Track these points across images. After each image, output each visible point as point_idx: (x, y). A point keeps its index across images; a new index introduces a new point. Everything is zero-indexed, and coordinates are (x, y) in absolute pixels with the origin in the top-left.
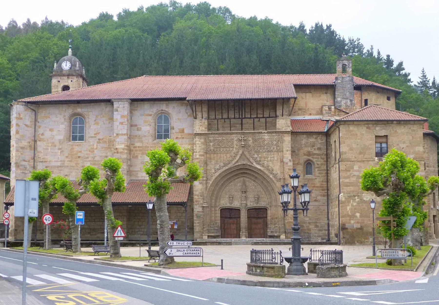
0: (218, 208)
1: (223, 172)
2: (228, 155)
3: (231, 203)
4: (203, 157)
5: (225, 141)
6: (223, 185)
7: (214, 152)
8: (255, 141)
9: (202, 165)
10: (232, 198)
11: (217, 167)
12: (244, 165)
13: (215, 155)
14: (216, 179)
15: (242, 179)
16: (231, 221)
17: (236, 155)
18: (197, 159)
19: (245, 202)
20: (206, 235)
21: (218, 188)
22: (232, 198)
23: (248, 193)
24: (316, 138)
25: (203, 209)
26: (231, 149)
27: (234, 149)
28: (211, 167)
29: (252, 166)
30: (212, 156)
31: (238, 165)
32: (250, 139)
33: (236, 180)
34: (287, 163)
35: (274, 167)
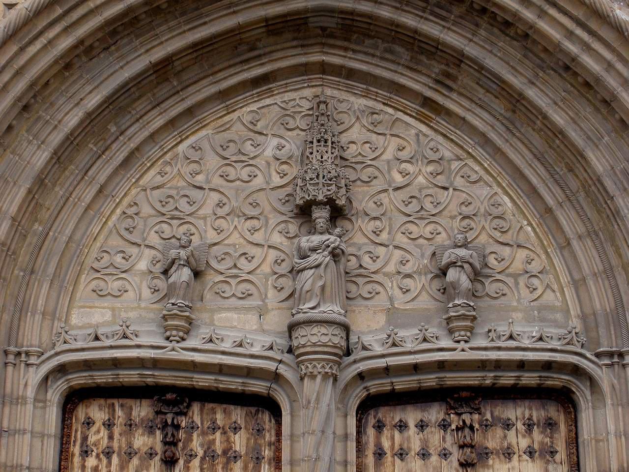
0: (35, 376)
3: (178, 323)
6: (95, 124)
10: (189, 273)
15: (300, 96)
19: (332, 309)
21: (41, 158)
22: (189, 273)
23: (358, 235)
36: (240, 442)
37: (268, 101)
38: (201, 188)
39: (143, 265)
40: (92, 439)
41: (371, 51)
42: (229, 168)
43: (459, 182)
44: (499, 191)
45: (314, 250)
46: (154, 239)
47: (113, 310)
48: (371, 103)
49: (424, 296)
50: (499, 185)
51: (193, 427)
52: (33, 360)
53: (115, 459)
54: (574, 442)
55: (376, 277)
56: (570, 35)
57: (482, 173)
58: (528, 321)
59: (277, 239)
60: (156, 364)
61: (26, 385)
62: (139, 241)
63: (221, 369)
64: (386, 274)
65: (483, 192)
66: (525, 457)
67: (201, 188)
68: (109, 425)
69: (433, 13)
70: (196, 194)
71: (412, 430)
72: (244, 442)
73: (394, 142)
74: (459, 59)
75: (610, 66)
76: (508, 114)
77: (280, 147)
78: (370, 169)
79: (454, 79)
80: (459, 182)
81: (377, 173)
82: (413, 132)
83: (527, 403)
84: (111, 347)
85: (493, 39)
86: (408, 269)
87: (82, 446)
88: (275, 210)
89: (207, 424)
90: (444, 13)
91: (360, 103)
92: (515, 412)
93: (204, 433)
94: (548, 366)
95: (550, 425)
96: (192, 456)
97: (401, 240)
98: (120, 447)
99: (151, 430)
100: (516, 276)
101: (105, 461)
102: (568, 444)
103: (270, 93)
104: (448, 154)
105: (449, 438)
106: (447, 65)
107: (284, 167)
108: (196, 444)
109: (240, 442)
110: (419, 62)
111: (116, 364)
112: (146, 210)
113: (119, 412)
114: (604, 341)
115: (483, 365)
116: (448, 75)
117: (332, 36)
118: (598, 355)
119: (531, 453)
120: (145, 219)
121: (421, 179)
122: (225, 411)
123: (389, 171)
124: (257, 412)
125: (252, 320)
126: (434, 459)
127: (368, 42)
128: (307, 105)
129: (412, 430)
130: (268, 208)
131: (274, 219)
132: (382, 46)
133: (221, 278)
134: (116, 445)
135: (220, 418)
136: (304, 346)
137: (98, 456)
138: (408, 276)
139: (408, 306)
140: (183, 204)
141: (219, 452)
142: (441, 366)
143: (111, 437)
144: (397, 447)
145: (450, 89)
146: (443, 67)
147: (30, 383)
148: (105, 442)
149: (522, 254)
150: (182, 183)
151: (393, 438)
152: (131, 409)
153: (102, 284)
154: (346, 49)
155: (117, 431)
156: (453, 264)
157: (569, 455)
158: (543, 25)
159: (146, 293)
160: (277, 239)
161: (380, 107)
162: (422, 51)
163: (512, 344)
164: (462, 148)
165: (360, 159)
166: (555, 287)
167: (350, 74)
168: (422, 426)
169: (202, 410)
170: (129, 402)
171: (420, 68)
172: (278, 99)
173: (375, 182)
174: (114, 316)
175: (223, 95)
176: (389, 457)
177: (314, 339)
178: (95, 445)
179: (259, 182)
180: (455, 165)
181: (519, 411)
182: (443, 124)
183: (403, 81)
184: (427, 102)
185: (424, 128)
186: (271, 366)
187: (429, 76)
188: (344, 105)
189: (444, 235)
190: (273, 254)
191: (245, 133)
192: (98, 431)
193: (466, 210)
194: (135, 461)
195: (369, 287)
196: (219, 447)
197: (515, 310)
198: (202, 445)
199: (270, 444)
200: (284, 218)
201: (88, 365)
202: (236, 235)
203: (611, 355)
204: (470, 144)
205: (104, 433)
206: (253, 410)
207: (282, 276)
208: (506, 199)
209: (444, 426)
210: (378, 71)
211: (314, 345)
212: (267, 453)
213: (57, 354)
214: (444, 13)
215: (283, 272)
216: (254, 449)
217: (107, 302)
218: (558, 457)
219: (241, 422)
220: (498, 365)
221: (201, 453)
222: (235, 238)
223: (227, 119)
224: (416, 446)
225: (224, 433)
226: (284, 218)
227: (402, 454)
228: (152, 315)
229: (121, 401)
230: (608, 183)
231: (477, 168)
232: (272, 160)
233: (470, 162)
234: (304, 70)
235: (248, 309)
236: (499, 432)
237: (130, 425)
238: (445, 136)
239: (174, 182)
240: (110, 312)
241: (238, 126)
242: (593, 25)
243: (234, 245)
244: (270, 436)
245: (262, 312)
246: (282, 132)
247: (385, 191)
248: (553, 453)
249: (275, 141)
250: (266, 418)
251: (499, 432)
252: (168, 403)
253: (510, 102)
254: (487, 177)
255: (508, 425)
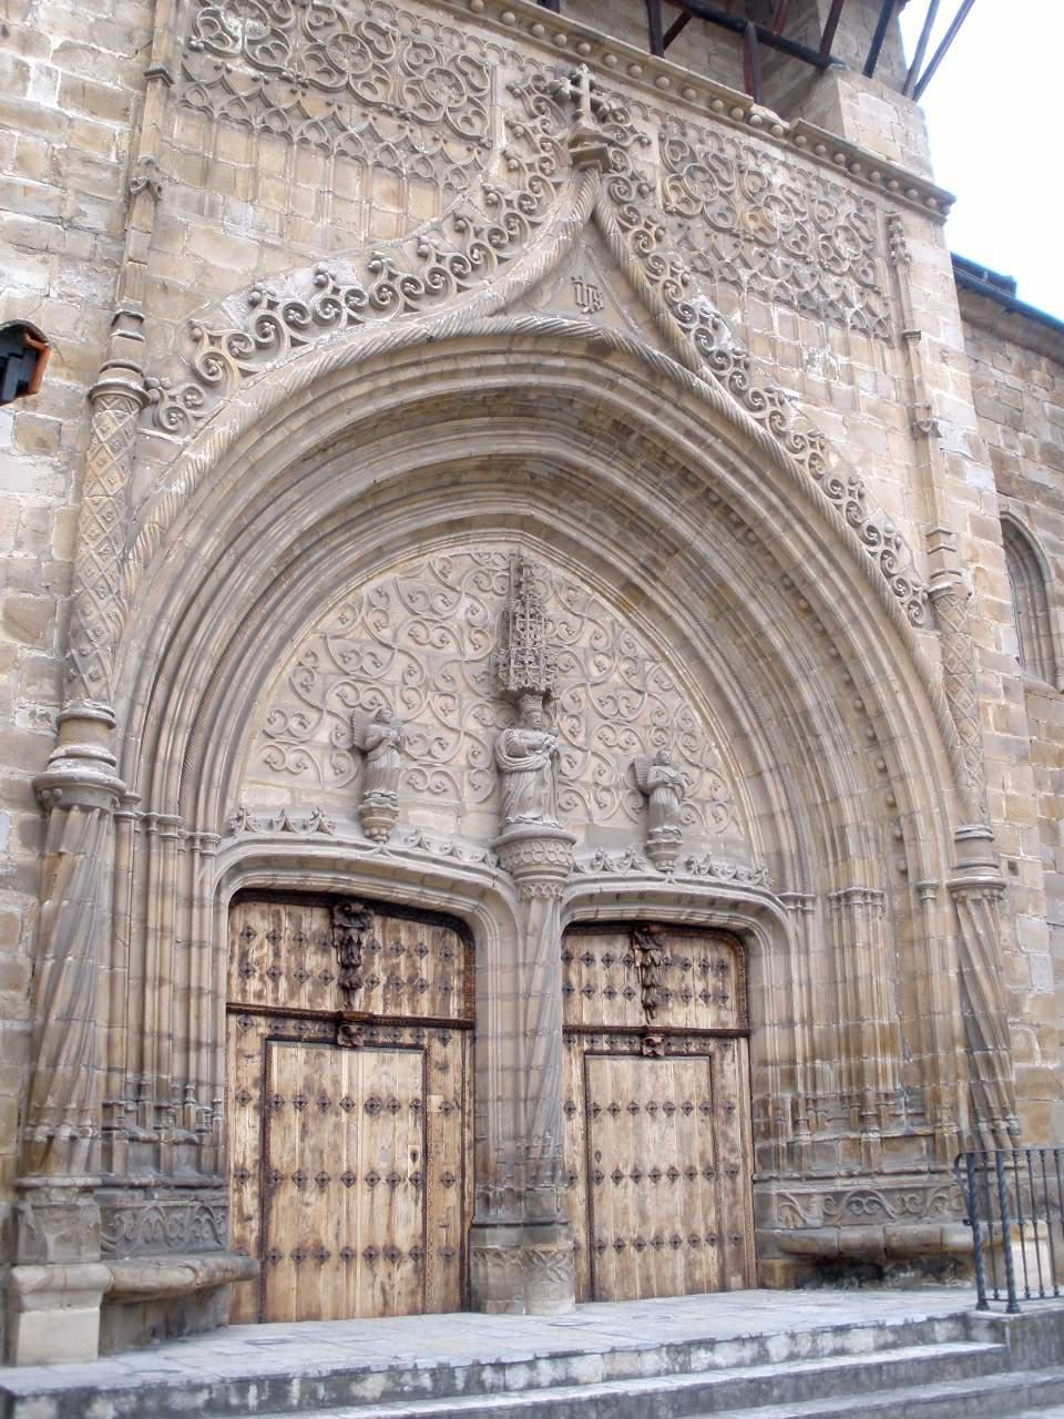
1: (363, 364)
2: (424, 206)
4: (115, 126)
5: (399, 52)
7: (264, 116)
8: (680, 160)
9: (96, 217)
11: (295, 286)
12: (600, 349)
13: (272, 156)
14: (267, 420)
15: (496, 550)
16: (360, 1071)
17: (518, 220)
18: (33, 119)
20: (70, 1293)
24: (1023, 373)
25: (40, 835)
26: (456, 151)
27: (496, 167)
28: (204, 270)
29: (685, 388)
30: (232, 147)
31: (541, 335)
32: (651, 132)
33: (441, 553)
34: (955, 468)
35: (865, 461)
36: (427, 968)
37: (461, 550)
38: (388, 647)
39: (323, 736)
40: (254, 955)
41: (580, 515)
42: (419, 628)
43: (652, 686)
44: (690, 703)
45: (533, 749)
46: (337, 706)
47: (292, 790)
48: (569, 576)
49: (620, 815)
50: (691, 696)
51: (373, 947)
52: (211, 850)
53: (283, 984)
54: (744, 989)
55: (576, 787)
56: (810, 556)
57: (675, 680)
58: (721, 855)
59: (472, 725)
60: (350, 867)
61: (202, 882)
62: (317, 702)
63: (424, 880)
64: (584, 784)
65: (673, 702)
66: (701, 1001)
67: (388, 647)
68: (274, 938)
69: (662, 491)
70: (383, 654)
71: (599, 965)
72: (432, 970)
73: (589, 628)
74: (675, 547)
75: (842, 599)
76: (712, 620)
77: (473, 611)
78: (567, 656)
79: (662, 568)
80: (652, 686)
81: (574, 663)
82: (609, 619)
83: (702, 942)
84: (308, 842)
85: (719, 535)
86: (604, 780)
87: (241, 963)
88: (469, 688)
89: (390, 944)
90: (674, 495)
91: (559, 573)
92: (694, 951)
93: (386, 956)
94: (735, 905)
95: (723, 967)
96: (374, 982)
97: (597, 745)
98: (288, 968)
99: (324, 947)
100: (703, 803)
101: (270, 984)
102: (738, 990)
103: (465, 540)
104: (641, 652)
105: (633, 977)
106: (656, 550)
107: (479, 636)
108: (378, 968)
109: (427, 968)
110: (627, 539)
111: (303, 863)
112: (325, 665)
113: (286, 923)
114: (790, 884)
115: (678, 899)
116: (655, 561)
117: (539, 486)
118: (782, 898)
119: (706, 997)
120: (325, 676)
121: (616, 677)
122: (410, 930)
123: (586, 660)
124: (445, 933)
125: (448, 823)
126: (619, 998)
127: (578, 503)
128: (502, 564)
129: (599, 965)
130: (461, 685)
131: (469, 701)
132: (591, 511)
133: (414, 765)
134: (283, 965)
135: (404, 936)
136: (539, 864)
137: (261, 977)
138: (607, 789)
139: (607, 824)
140: (367, 662)
141: (404, 979)
142: (642, 897)
143: (277, 955)
144: (584, 984)
145: (656, 578)
146: (651, 551)
147: (208, 879)
148: (269, 961)
149: (709, 779)
150: (366, 637)
151: (580, 973)
152: (300, 918)
153: (276, 755)
154: (551, 505)
155: (284, 946)
156: (664, 784)
157: (738, 1002)
158: (788, 541)
159: (328, 773)
160: (472, 725)
161: (577, 582)
162: (633, 527)
163: (712, 879)
164: (657, 647)
165: (556, 641)
166: (739, 819)
167: (551, 535)
168: (608, 960)
169: (383, 926)
170: (299, 910)
171: (629, 548)
172: (471, 549)
173: (572, 673)
174: (293, 798)
175: (418, 536)
176: (576, 995)
177: (552, 858)
178: (259, 962)
179: (451, 648)
180: (649, 665)
181: (696, 951)
182: (644, 617)
183: (612, 559)
184: (628, 586)
185: (621, 618)
186: (487, 882)
187: (635, 559)
188: (541, 571)
189: (638, 745)
190: (467, 743)
191: (434, 584)
192: (261, 946)
193: (660, 721)
194: (308, 987)
195: (567, 796)
196: (404, 974)
197: (704, 840)
198: (385, 970)
199: (459, 973)
200: (481, 701)
201: (267, 862)
202: (428, 713)
203: (795, 900)
204: (668, 644)
205: (268, 949)
206: (440, 930)
207: (479, 771)
208: (697, 714)
209: (629, 962)
210: (586, 542)
211: (552, 864)
212: (456, 983)
213: (240, 844)
214: (674, 495)
215: (482, 767)
216: (442, 977)
217: (284, 780)
218: (728, 1003)
219: (427, 944)
220: (692, 900)
221: (383, 979)
222: (426, 717)
223: (416, 562)
224: (602, 984)
225: (410, 956)
226: (481, 701)
227: (589, 991)
228: (338, 804)
229: (288, 908)
230: (816, 719)
231: (671, 674)
232: (464, 625)
233: (664, 666)
234: (503, 521)
235: (445, 808)
236: (678, 972)
237: (300, 940)
238: (639, 629)
239: (357, 633)
240: (285, 796)
241: (426, 575)
242: (837, 553)
243: (426, 726)
244: (458, 963)
245: (460, 813)
246: (475, 591)
247: (583, 685)
248: (725, 998)
249: (466, 602)
250: (453, 939)
251: (678, 972)
252: (350, 915)
253: (717, 607)
254: (680, 688)
255: (686, 966)
